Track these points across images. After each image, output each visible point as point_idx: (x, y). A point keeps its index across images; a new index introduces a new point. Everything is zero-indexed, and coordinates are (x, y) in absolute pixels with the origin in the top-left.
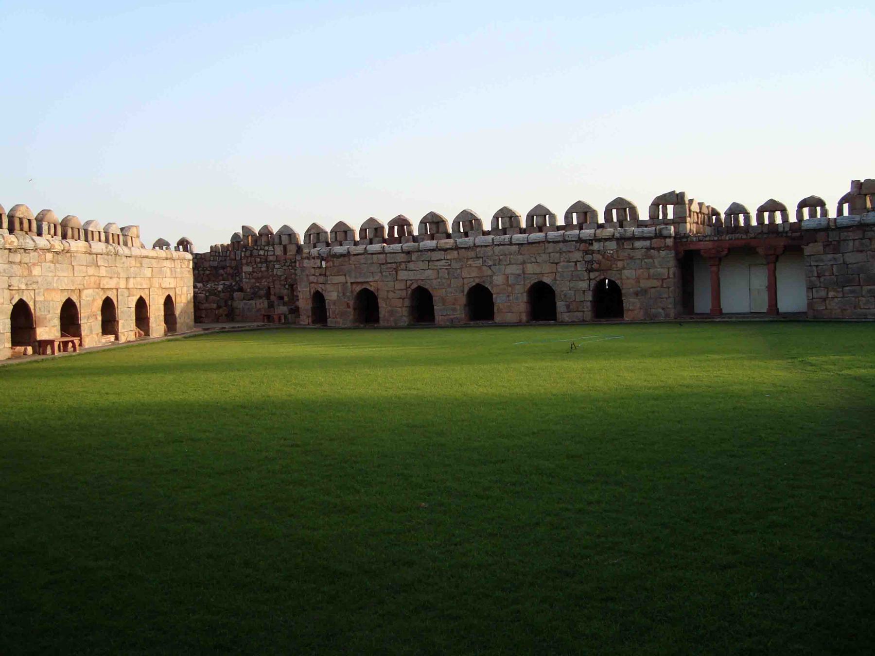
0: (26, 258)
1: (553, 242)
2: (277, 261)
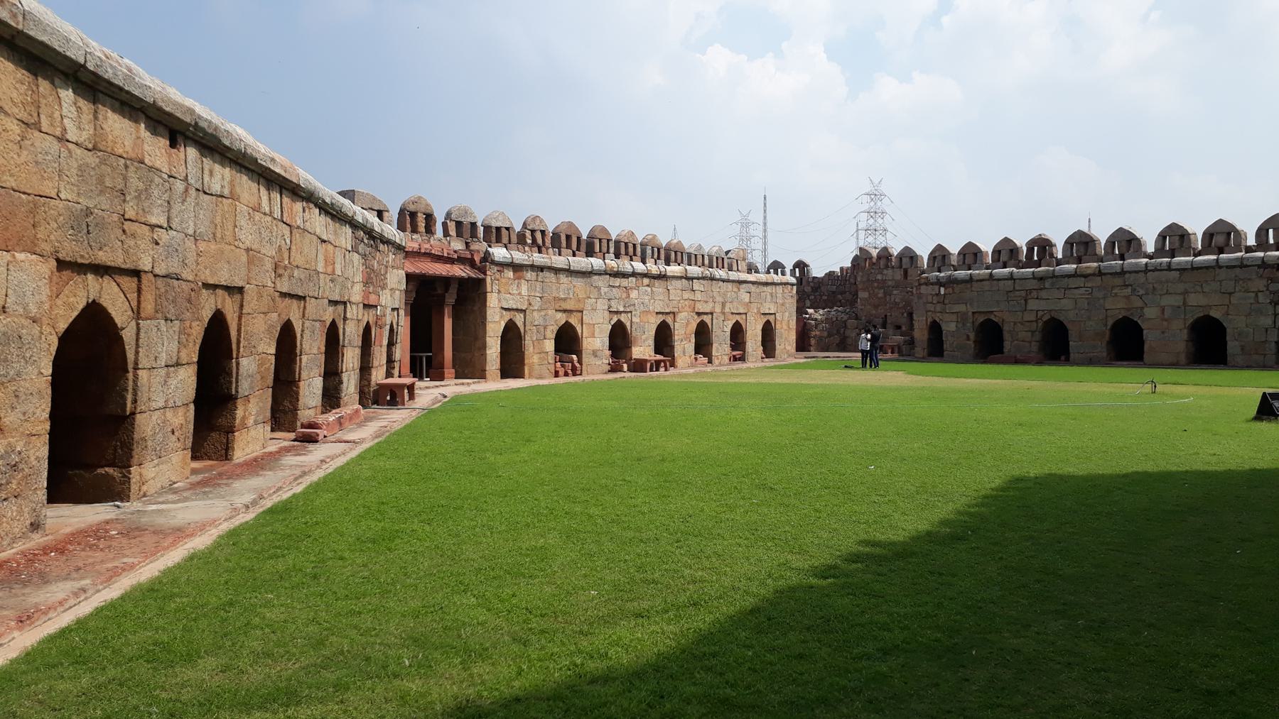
0: (624, 282)
1: (1227, 267)
2: (896, 287)
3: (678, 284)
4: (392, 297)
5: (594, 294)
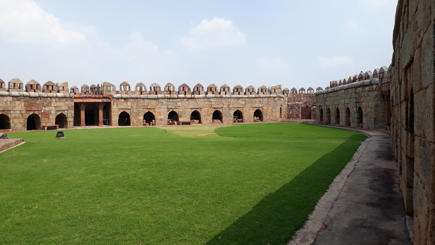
0: (175, 100)
3: (203, 100)
5: (161, 104)
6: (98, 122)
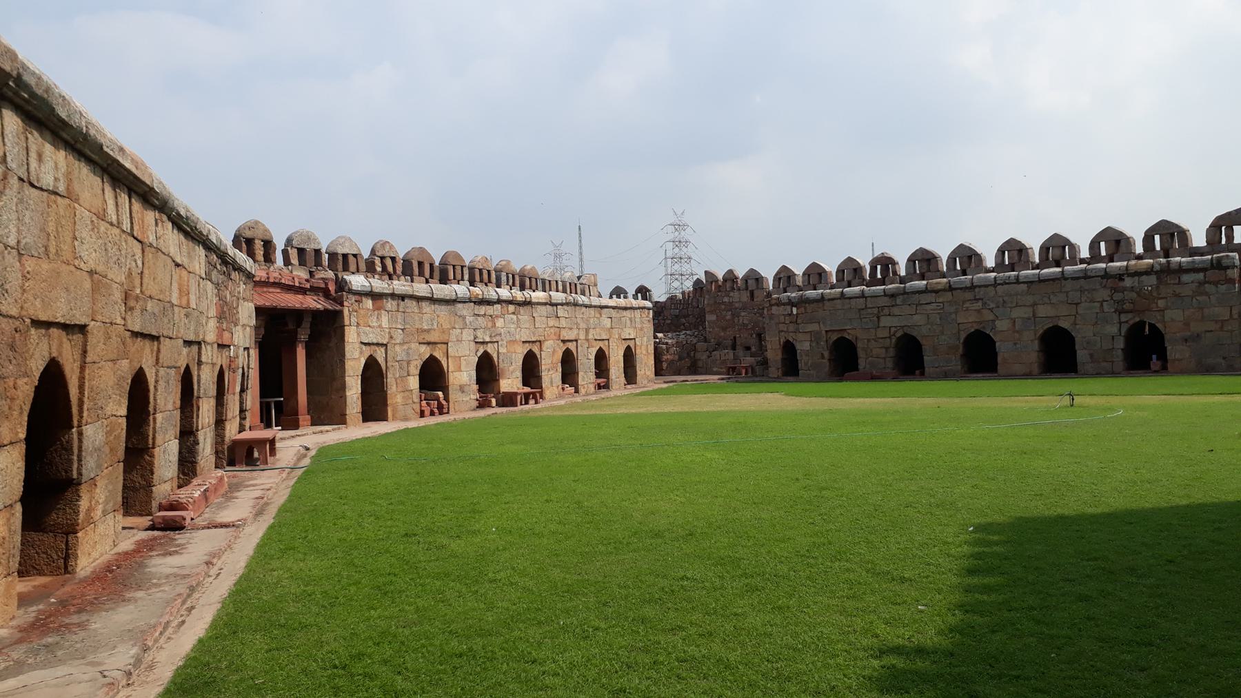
0: (490, 310)
1: (1073, 279)
2: (744, 308)
4: (243, 336)
6: (296, 413)
